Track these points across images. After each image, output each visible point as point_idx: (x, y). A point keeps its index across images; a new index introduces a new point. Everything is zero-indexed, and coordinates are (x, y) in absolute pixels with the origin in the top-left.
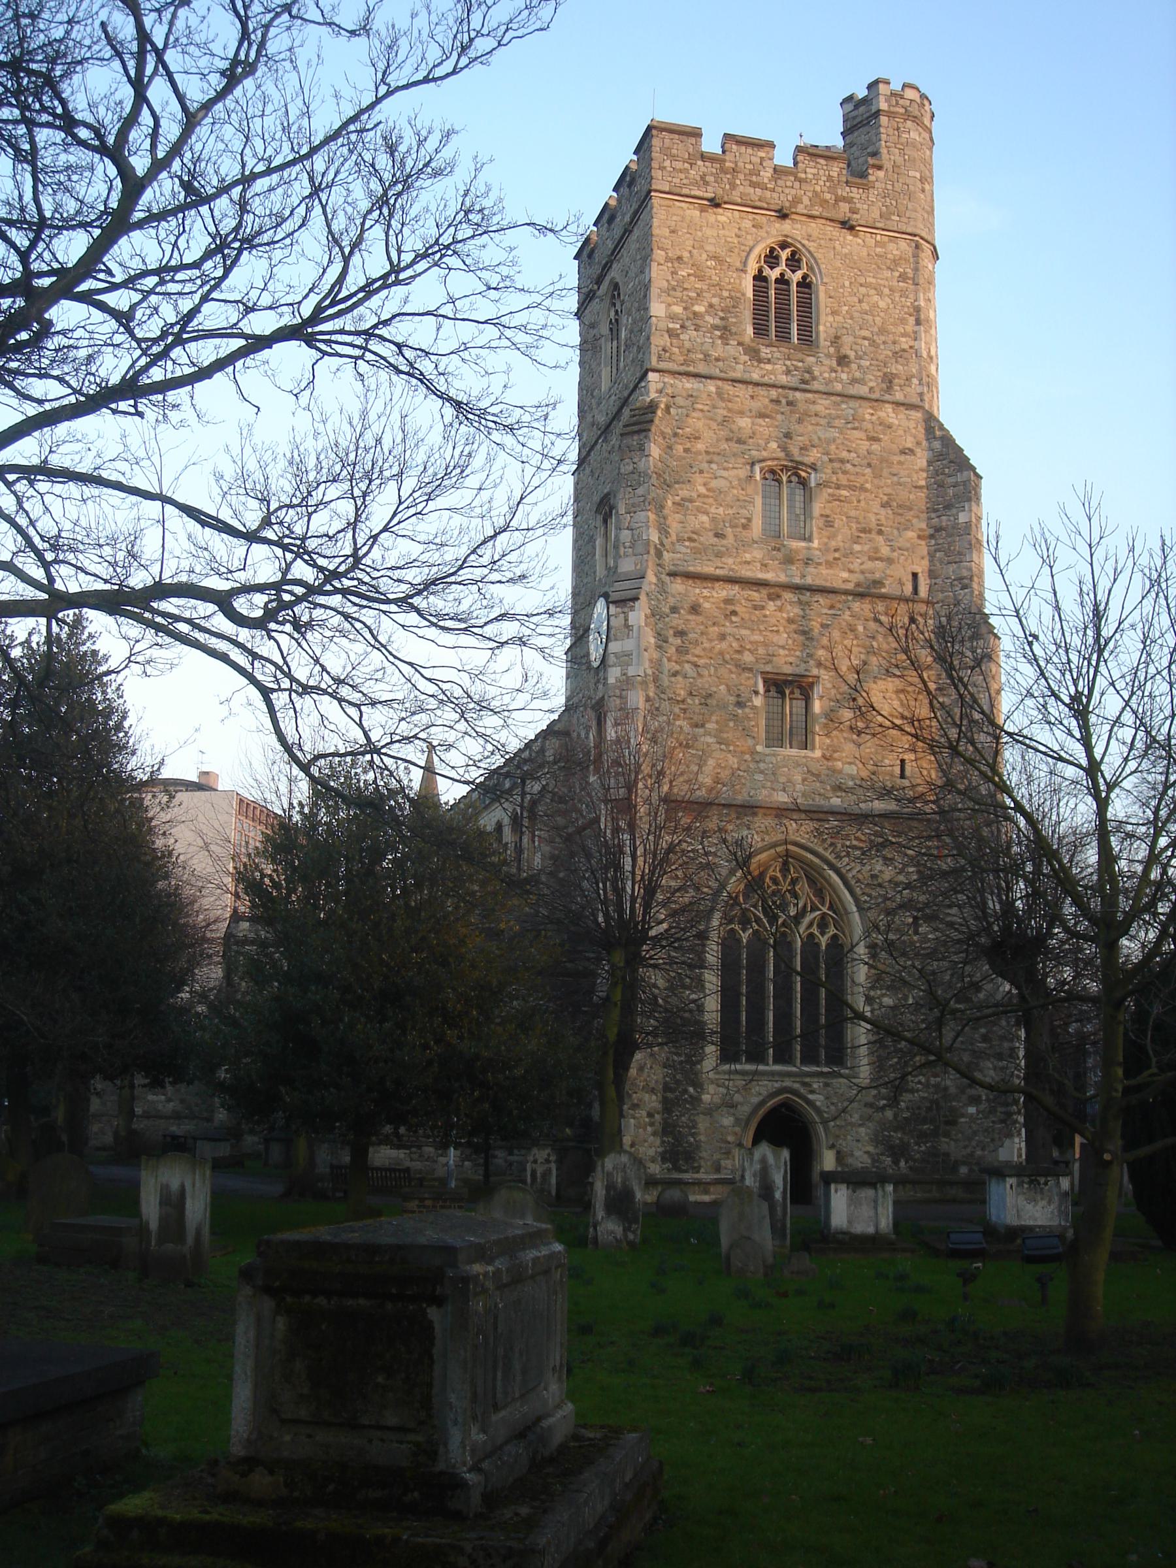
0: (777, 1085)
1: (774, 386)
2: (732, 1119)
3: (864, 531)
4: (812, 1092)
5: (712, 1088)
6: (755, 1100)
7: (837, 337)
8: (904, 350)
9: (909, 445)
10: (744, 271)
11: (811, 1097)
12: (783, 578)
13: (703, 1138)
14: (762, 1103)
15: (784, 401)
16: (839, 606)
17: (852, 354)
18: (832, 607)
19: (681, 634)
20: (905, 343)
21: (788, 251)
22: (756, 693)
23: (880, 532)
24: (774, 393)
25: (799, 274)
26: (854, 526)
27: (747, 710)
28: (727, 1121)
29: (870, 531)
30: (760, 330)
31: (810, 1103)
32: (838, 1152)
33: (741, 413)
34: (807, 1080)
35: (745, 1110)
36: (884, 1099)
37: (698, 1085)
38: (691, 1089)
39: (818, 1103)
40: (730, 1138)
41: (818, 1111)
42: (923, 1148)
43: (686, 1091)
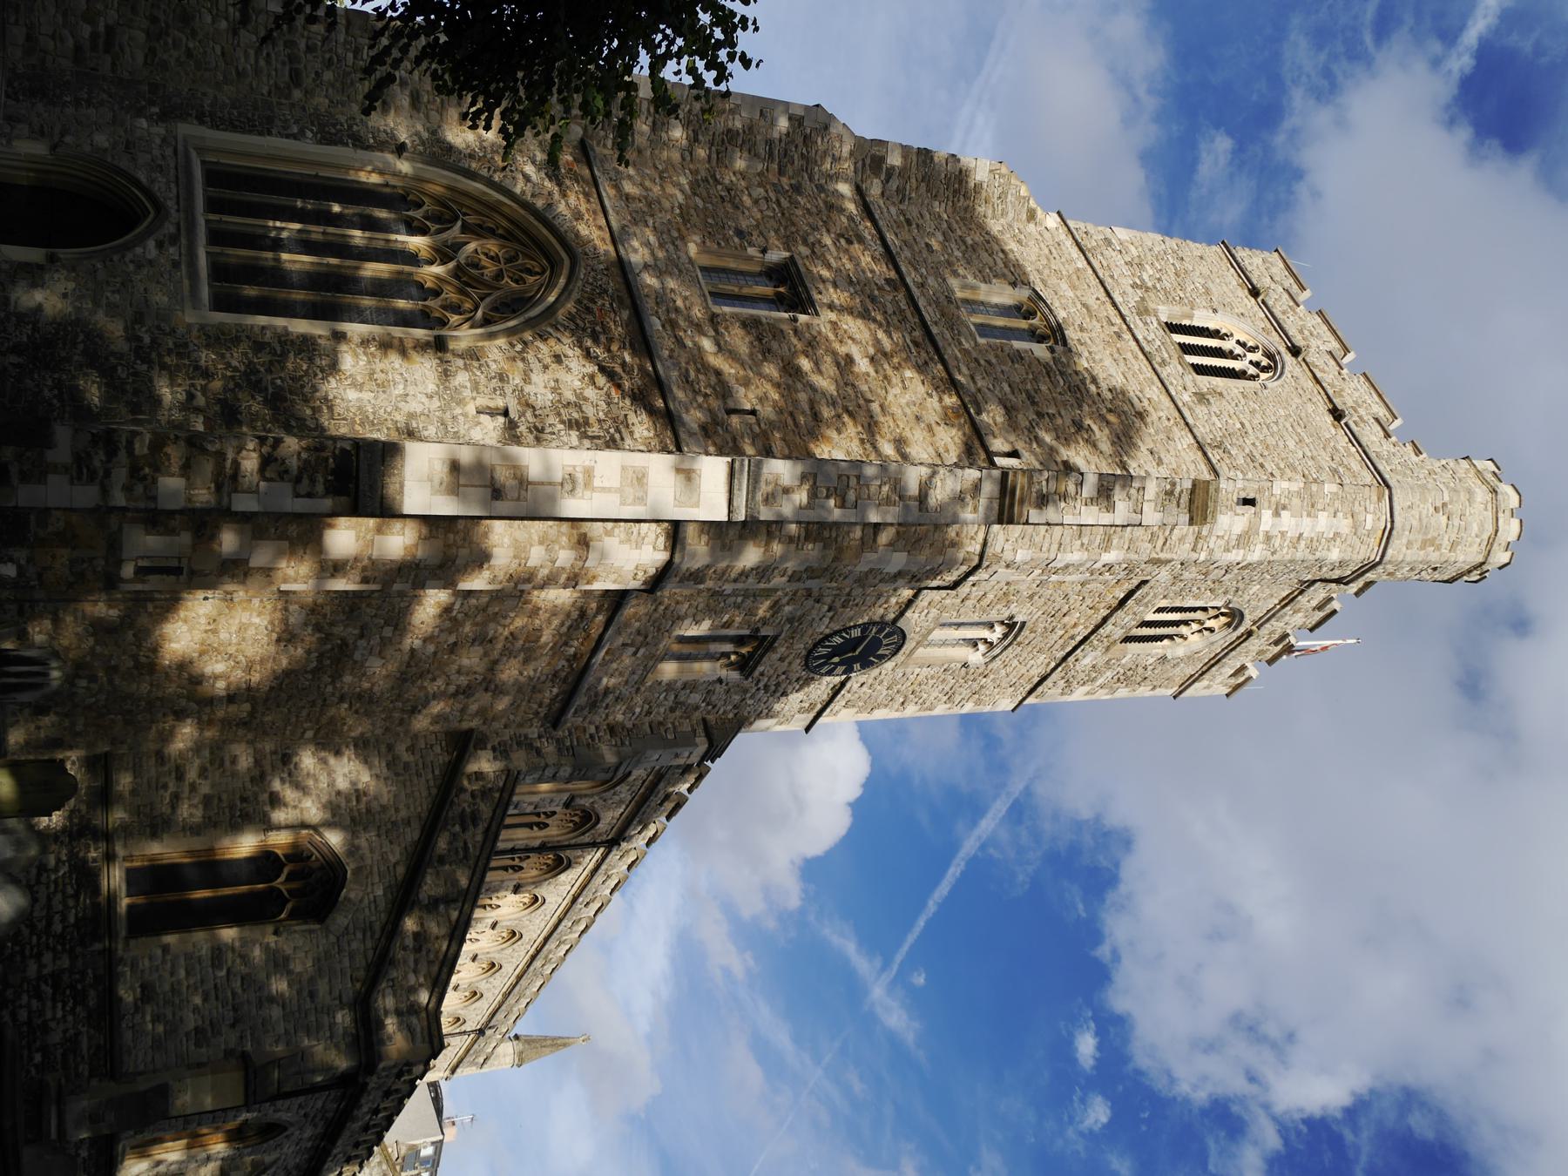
0: (171, 204)
1: (1124, 320)
2: (106, 145)
3: (1029, 397)
4: (160, 245)
5: (160, 130)
6: (142, 176)
7: (1221, 394)
8: (1262, 466)
9: (1165, 460)
10: (1215, 311)
11: (151, 244)
12: (922, 303)
13: (70, 110)
14: (137, 183)
15: (1116, 329)
16: (924, 355)
17: (1214, 408)
18: (916, 344)
19: (797, 189)
20: (1270, 466)
21: (1265, 362)
22: (764, 251)
23: (1040, 415)
24: (1118, 321)
25: (1252, 370)
26: (1029, 386)
27: (736, 240)
28: (101, 140)
29: (1034, 403)
30: (1174, 328)
31: (140, 240)
32: (40, 267)
33: (1074, 288)
34: (183, 241)
35: (124, 163)
36: (153, 341)
37: (164, 117)
38: (156, 110)
39: (139, 250)
40: (68, 139)
41: (128, 247)
42: (46, 393)
43: (152, 103)
